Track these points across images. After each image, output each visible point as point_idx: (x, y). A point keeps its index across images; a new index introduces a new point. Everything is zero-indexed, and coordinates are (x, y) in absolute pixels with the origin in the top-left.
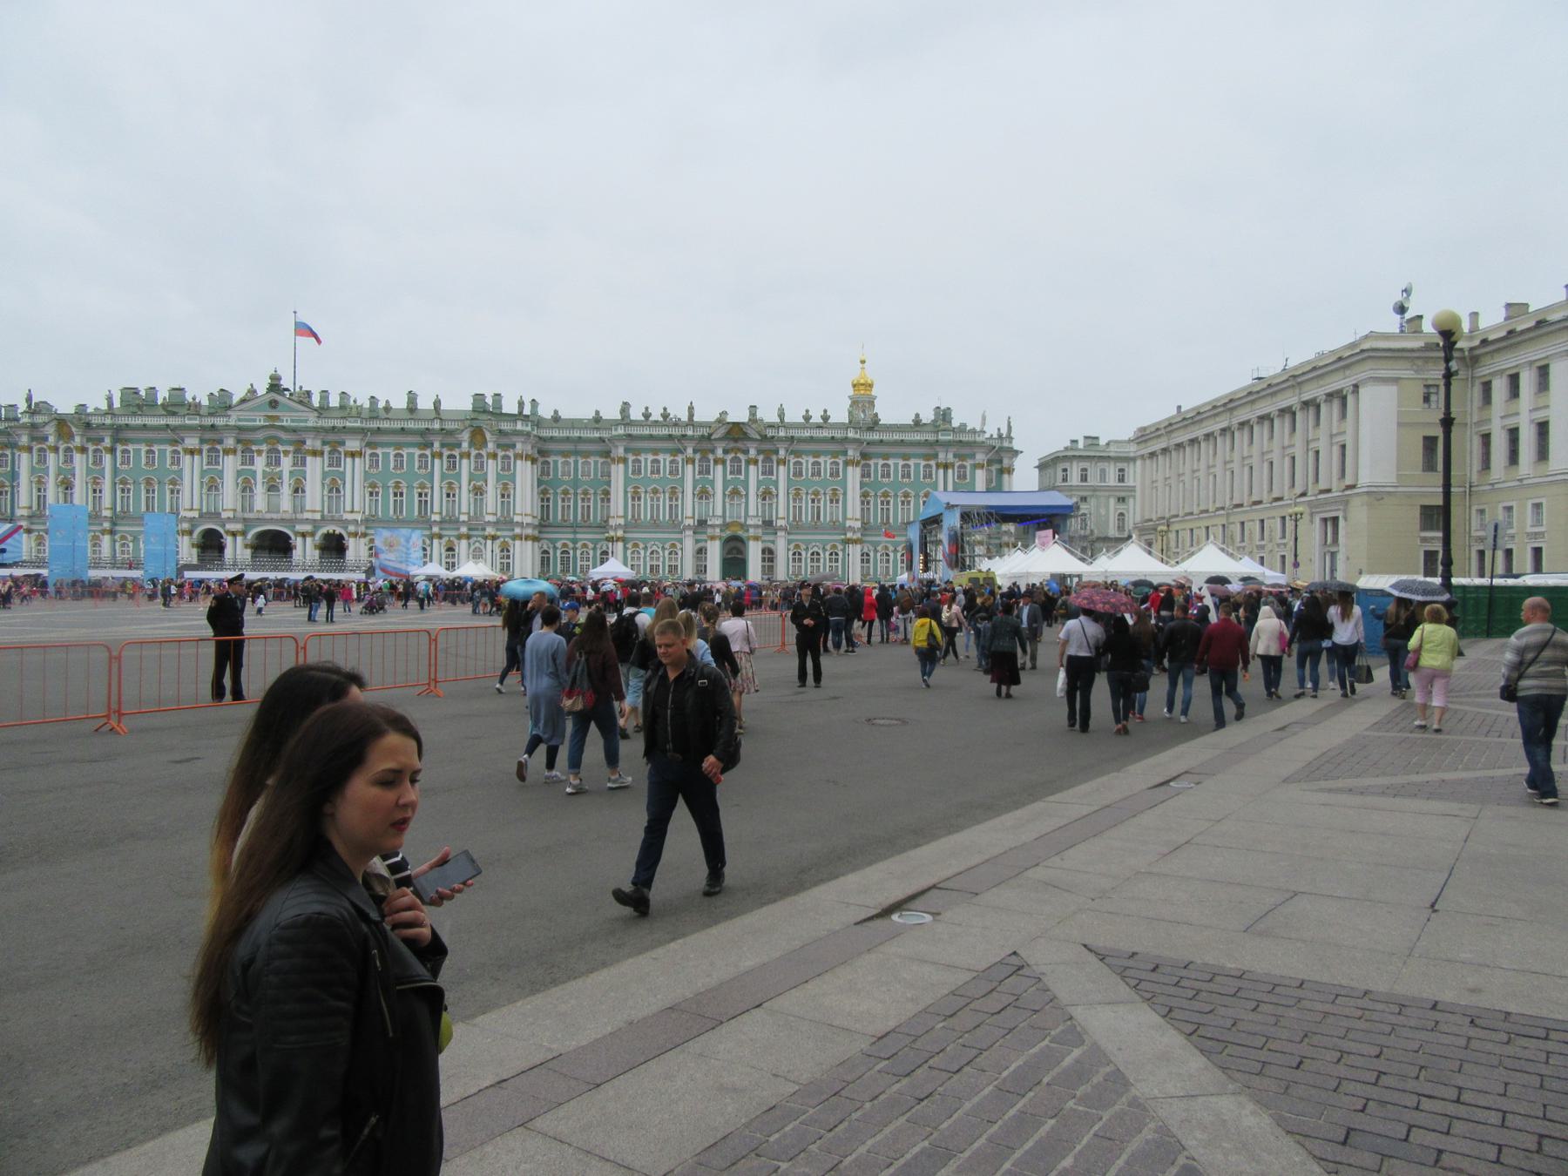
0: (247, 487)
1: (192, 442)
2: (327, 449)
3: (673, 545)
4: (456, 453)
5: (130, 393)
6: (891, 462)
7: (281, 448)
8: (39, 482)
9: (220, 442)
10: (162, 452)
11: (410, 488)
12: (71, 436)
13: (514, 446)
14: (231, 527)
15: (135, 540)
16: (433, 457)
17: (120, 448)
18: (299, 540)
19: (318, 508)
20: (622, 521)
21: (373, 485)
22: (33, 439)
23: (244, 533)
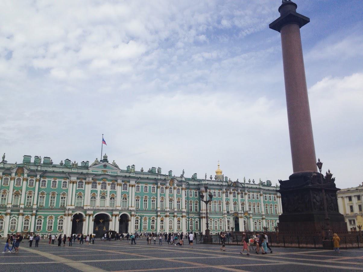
0: (93, 197)
2: (123, 183)
4: (164, 187)
5: (27, 158)
6: (267, 195)
7: (107, 182)
9: (85, 179)
12: (23, 174)
13: (181, 186)
14: (88, 212)
16: (157, 187)
17: (42, 179)
18: (114, 217)
19: (120, 206)
21: (138, 197)
23: (93, 215)
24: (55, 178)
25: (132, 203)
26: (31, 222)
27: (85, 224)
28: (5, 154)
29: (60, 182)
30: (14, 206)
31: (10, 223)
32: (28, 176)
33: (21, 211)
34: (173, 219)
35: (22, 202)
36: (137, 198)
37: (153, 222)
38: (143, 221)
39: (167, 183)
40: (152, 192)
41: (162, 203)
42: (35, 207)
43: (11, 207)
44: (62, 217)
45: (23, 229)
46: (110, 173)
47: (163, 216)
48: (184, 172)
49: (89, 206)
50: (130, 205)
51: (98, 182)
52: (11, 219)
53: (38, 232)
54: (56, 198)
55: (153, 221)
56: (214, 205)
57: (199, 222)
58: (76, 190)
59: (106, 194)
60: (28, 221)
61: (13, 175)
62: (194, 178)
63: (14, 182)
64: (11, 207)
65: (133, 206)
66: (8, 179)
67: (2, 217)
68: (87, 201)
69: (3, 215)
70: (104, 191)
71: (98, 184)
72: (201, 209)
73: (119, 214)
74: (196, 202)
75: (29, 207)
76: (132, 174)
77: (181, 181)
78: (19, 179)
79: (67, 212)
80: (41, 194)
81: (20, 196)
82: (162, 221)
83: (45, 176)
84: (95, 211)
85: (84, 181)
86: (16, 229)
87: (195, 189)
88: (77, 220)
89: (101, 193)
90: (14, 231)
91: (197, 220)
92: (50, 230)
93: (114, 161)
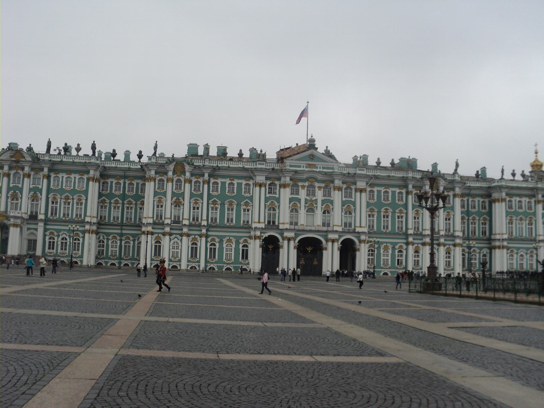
0: (294, 210)
1: (261, 179)
2: (345, 186)
3: (532, 252)
8: (160, 201)
9: (279, 179)
10: (239, 185)
11: (394, 213)
12: (184, 173)
13: (453, 189)
15: (221, 242)
16: (408, 193)
17: (212, 180)
18: (330, 244)
19: (340, 224)
20: (505, 236)
21: (372, 210)
22: (156, 173)
23: (294, 239)
24: (232, 178)
25: (362, 220)
27: (283, 253)
29: (239, 185)
30: (175, 222)
31: (171, 247)
32: (192, 175)
33: (185, 230)
34: (438, 249)
35: (186, 216)
36: (370, 211)
37: (400, 254)
38: (382, 251)
39: (425, 185)
40: (397, 202)
41: (417, 220)
42: (204, 223)
43: (170, 223)
44: (246, 241)
45: (190, 257)
46: (320, 168)
47: (418, 244)
48: (457, 165)
49: (288, 223)
50: (358, 224)
51: (300, 184)
52: (172, 242)
53: (212, 263)
54: (235, 210)
55: (400, 251)
56: (519, 224)
57: (488, 255)
58: (266, 198)
59: (315, 205)
60: (196, 244)
61: (170, 174)
62: (480, 176)
63: (173, 185)
64: (170, 223)
65: (363, 225)
66: (163, 181)
67: (160, 238)
68: (284, 217)
70: (311, 201)
71: (300, 188)
72: (493, 233)
73: (339, 239)
74: (484, 220)
76: (359, 170)
77: (452, 182)
78: (179, 181)
79: (252, 233)
80: (213, 204)
82: (417, 252)
84: (298, 232)
85: (277, 183)
86: (179, 256)
87: (482, 196)
88: (271, 247)
89: (306, 203)
90: (178, 259)
91: (485, 253)
92: (228, 260)
93: (327, 147)
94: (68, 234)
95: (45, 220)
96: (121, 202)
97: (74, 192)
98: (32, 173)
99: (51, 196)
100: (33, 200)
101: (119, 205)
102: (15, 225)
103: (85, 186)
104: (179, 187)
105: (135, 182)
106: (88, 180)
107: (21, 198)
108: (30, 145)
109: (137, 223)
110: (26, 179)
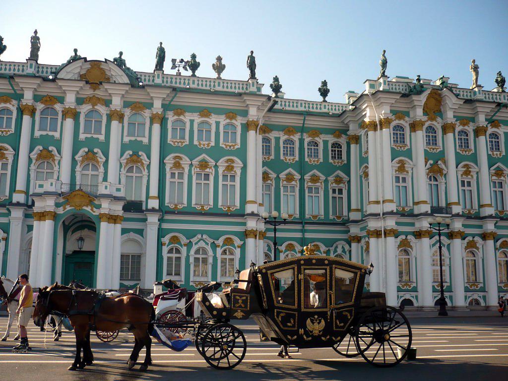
8: (402, 168)
17: (490, 130)
26: (483, 260)
28: (385, 51)
61: (419, 113)
64: (429, 212)
69: (409, 237)
75: (469, 212)
78: (431, 129)
81: (444, 181)
83: (497, 120)
94: (210, 241)
95: (160, 210)
96: (297, 176)
97: (217, 152)
98: (127, 112)
99: (169, 160)
100: (130, 170)
101: (293, 183)
102: (113, 219)
103: (238, 140)
104: (432, 140)
105: (320, 140)
106: (246, 127)
107: (106, 164)
108: (121, 53)
109: (331, 217)
110: (115, 124)
